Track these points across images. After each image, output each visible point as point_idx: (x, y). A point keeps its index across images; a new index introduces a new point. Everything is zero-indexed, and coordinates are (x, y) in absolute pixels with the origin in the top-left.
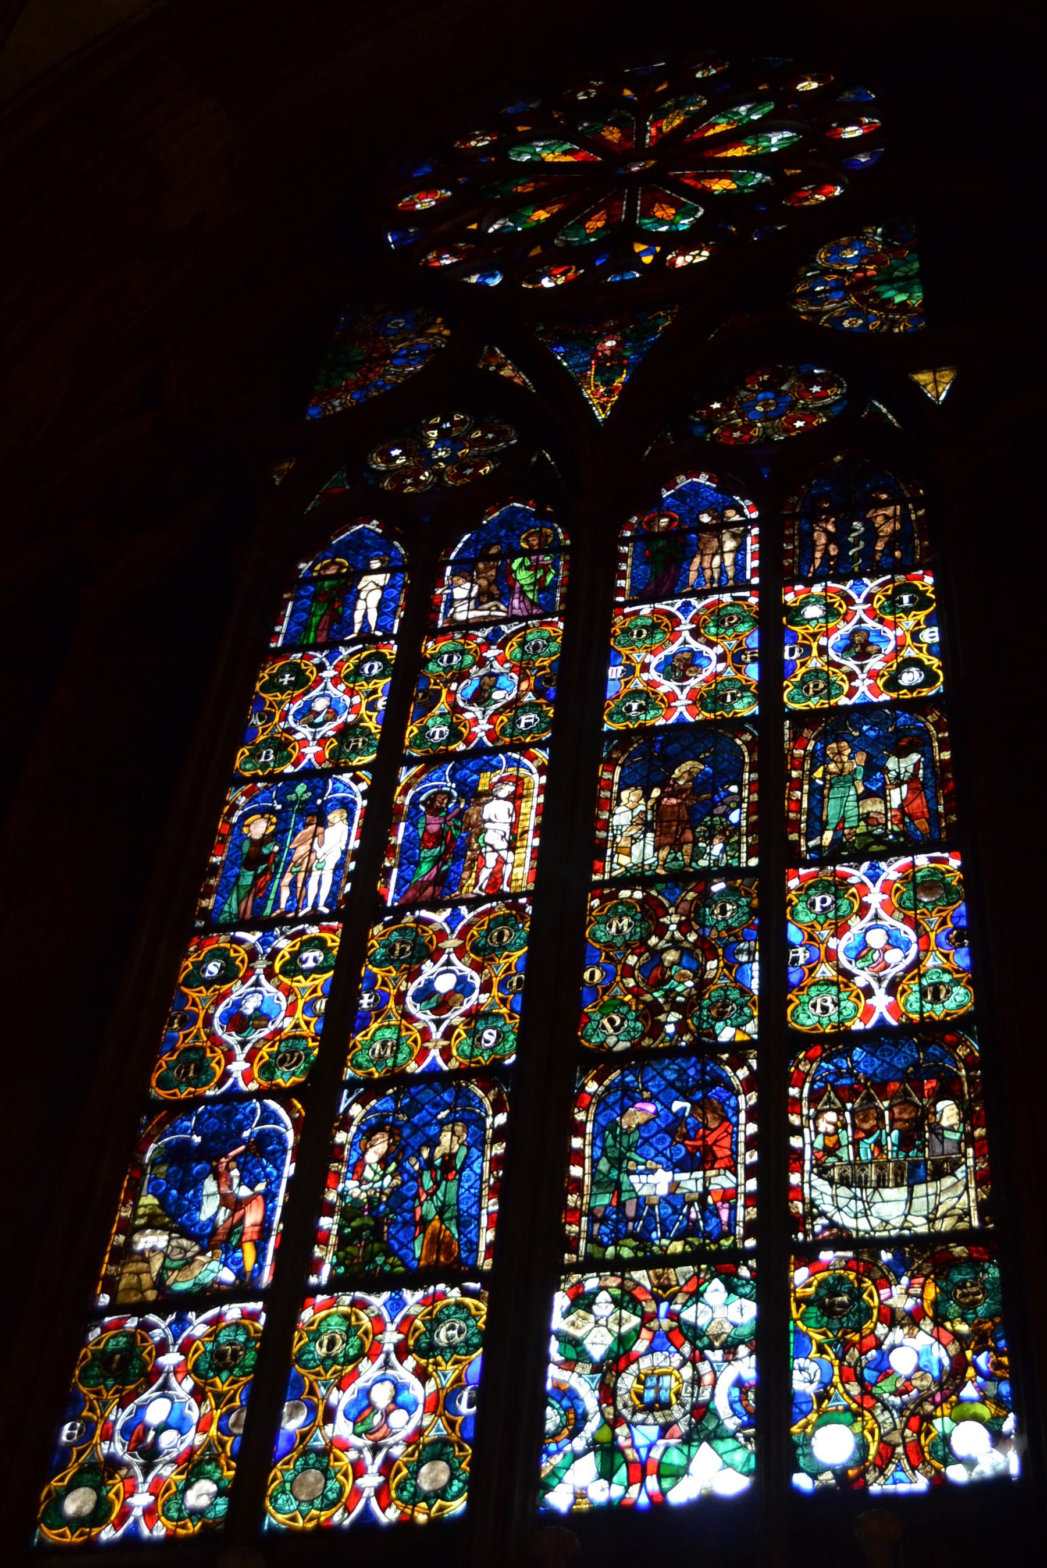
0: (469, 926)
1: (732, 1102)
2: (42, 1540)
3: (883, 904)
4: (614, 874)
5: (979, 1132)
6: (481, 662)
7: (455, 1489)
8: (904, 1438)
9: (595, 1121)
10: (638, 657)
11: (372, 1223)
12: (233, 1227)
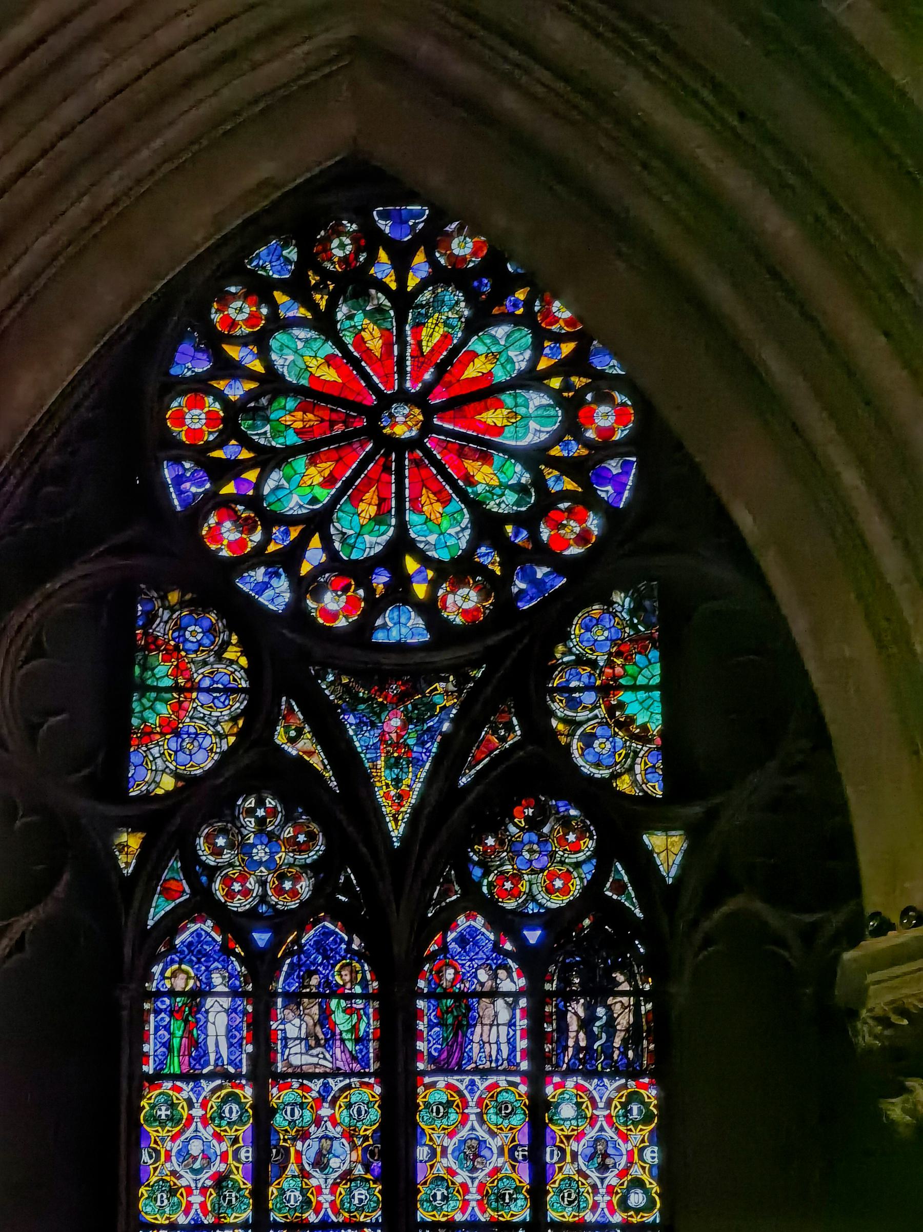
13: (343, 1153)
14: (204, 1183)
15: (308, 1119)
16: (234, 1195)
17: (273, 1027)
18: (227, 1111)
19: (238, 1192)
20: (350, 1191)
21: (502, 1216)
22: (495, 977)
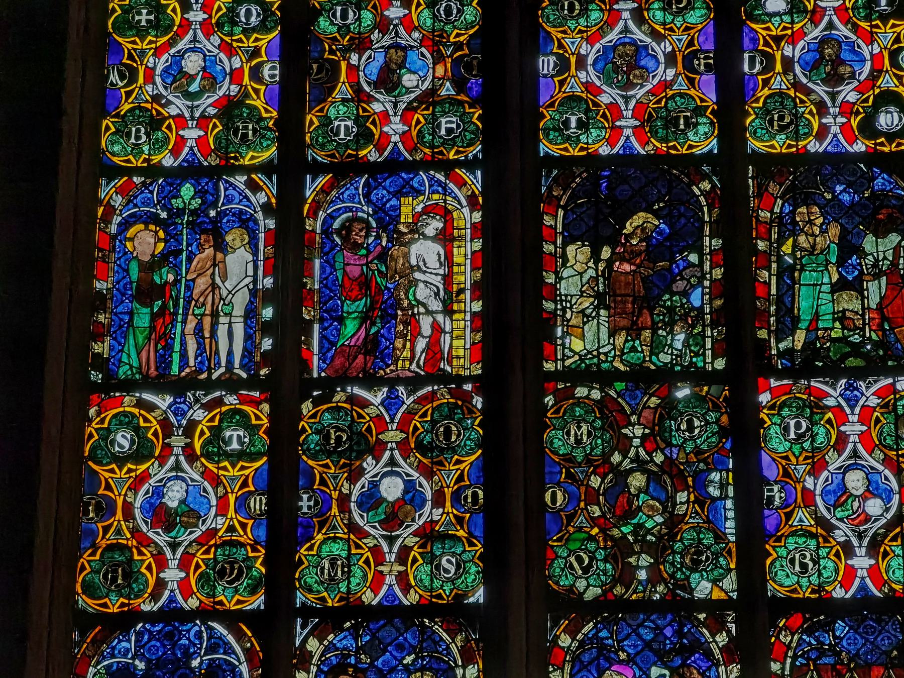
0: (410, 414)
3: (864, 437)
4: (567, 363)
6: (383, 25)
10: (574, 44)
13: (424, 67)
15: (369, 23)
16: (250, 127)
19: (257, 122)
20: (434, 122)
21: (674, 148)
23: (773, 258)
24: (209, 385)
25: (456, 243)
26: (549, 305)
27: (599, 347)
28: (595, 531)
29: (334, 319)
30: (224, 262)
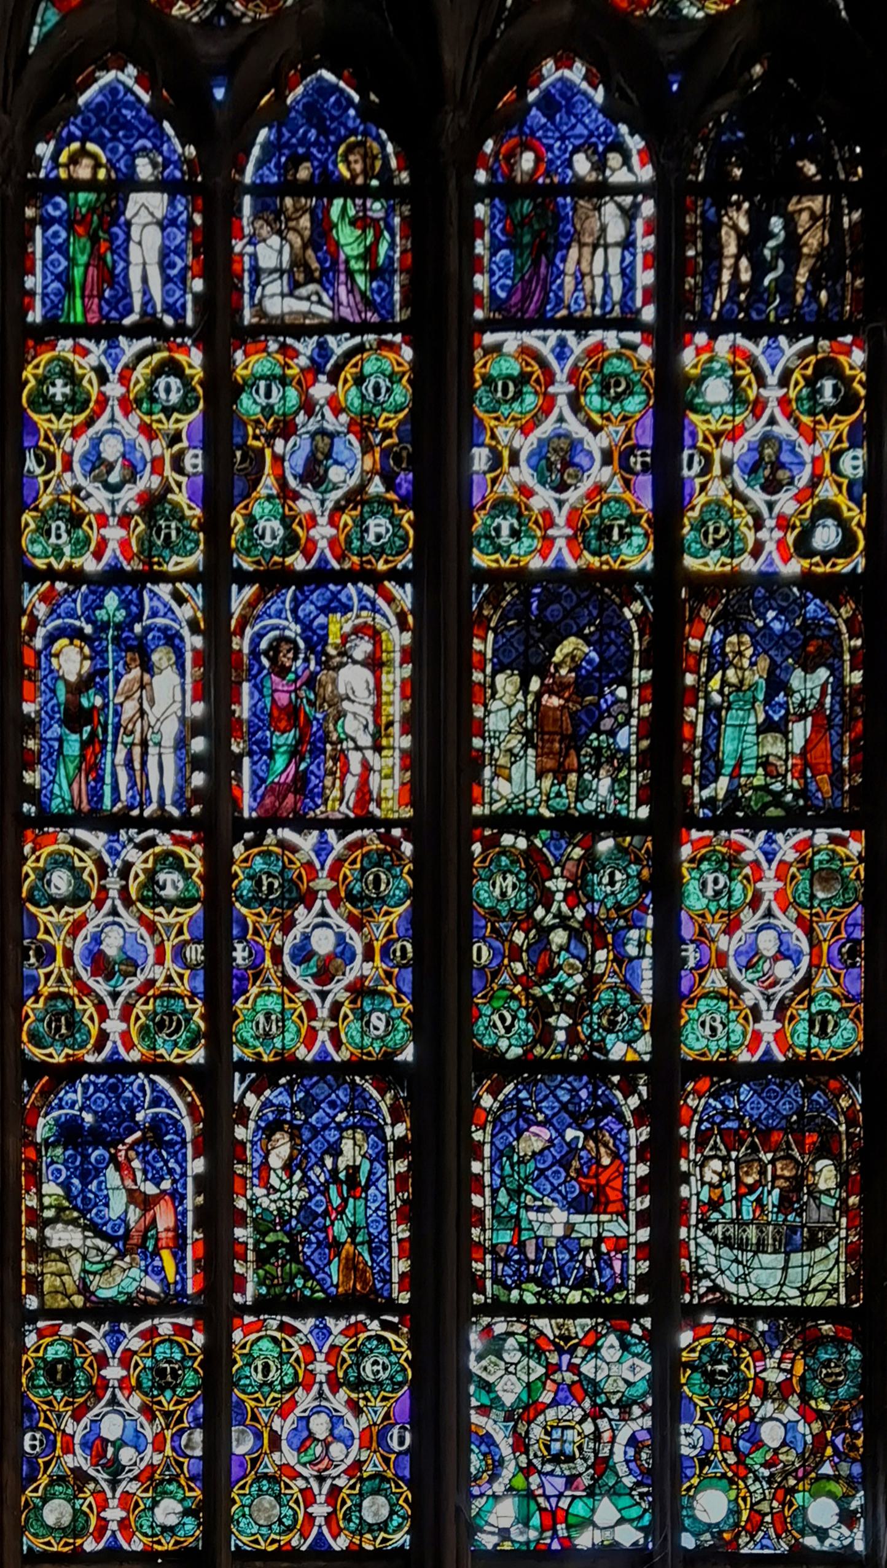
0: (339, 862)
1: (623, 1136)
2: (30, 1549)
4: (495, 807)
5: (853, 1200)
6: (308, 406)
7: (395, 1523)
8: (772, 1508)
9: (492, 1143)
10: (505, 433)
11: (287, 1241)
12: (147, 1229)
14: (125, 506)
17: (237, 249)
18: (161, 388)
20: (361, 524)
22: (600, 165)
23: (701, 694)
24: (142, 824)
25: (385, 669)
26: (477, 742)
27: (526, 791)
28: (518, 989)
29: (263, 752)
30: (151, 684)
